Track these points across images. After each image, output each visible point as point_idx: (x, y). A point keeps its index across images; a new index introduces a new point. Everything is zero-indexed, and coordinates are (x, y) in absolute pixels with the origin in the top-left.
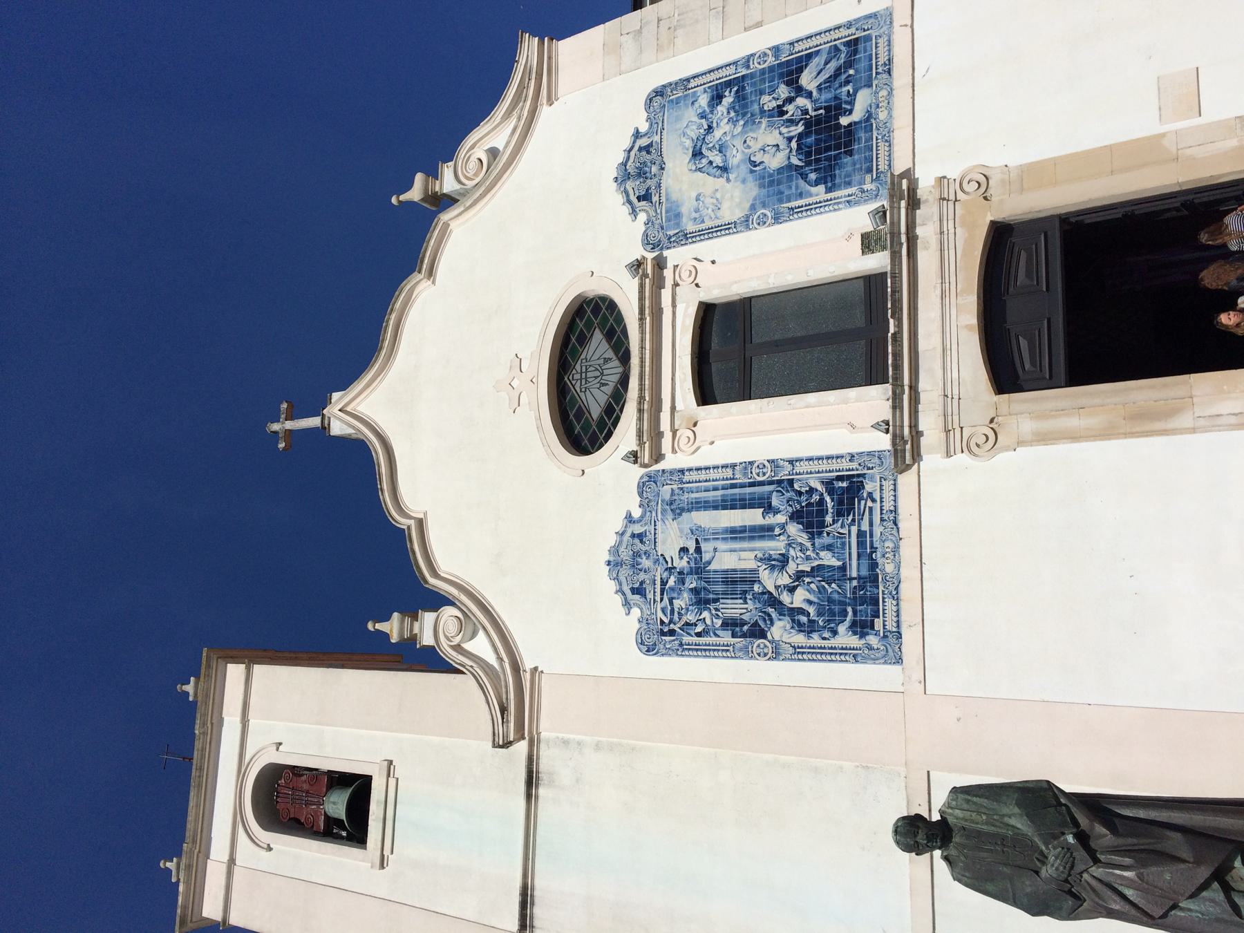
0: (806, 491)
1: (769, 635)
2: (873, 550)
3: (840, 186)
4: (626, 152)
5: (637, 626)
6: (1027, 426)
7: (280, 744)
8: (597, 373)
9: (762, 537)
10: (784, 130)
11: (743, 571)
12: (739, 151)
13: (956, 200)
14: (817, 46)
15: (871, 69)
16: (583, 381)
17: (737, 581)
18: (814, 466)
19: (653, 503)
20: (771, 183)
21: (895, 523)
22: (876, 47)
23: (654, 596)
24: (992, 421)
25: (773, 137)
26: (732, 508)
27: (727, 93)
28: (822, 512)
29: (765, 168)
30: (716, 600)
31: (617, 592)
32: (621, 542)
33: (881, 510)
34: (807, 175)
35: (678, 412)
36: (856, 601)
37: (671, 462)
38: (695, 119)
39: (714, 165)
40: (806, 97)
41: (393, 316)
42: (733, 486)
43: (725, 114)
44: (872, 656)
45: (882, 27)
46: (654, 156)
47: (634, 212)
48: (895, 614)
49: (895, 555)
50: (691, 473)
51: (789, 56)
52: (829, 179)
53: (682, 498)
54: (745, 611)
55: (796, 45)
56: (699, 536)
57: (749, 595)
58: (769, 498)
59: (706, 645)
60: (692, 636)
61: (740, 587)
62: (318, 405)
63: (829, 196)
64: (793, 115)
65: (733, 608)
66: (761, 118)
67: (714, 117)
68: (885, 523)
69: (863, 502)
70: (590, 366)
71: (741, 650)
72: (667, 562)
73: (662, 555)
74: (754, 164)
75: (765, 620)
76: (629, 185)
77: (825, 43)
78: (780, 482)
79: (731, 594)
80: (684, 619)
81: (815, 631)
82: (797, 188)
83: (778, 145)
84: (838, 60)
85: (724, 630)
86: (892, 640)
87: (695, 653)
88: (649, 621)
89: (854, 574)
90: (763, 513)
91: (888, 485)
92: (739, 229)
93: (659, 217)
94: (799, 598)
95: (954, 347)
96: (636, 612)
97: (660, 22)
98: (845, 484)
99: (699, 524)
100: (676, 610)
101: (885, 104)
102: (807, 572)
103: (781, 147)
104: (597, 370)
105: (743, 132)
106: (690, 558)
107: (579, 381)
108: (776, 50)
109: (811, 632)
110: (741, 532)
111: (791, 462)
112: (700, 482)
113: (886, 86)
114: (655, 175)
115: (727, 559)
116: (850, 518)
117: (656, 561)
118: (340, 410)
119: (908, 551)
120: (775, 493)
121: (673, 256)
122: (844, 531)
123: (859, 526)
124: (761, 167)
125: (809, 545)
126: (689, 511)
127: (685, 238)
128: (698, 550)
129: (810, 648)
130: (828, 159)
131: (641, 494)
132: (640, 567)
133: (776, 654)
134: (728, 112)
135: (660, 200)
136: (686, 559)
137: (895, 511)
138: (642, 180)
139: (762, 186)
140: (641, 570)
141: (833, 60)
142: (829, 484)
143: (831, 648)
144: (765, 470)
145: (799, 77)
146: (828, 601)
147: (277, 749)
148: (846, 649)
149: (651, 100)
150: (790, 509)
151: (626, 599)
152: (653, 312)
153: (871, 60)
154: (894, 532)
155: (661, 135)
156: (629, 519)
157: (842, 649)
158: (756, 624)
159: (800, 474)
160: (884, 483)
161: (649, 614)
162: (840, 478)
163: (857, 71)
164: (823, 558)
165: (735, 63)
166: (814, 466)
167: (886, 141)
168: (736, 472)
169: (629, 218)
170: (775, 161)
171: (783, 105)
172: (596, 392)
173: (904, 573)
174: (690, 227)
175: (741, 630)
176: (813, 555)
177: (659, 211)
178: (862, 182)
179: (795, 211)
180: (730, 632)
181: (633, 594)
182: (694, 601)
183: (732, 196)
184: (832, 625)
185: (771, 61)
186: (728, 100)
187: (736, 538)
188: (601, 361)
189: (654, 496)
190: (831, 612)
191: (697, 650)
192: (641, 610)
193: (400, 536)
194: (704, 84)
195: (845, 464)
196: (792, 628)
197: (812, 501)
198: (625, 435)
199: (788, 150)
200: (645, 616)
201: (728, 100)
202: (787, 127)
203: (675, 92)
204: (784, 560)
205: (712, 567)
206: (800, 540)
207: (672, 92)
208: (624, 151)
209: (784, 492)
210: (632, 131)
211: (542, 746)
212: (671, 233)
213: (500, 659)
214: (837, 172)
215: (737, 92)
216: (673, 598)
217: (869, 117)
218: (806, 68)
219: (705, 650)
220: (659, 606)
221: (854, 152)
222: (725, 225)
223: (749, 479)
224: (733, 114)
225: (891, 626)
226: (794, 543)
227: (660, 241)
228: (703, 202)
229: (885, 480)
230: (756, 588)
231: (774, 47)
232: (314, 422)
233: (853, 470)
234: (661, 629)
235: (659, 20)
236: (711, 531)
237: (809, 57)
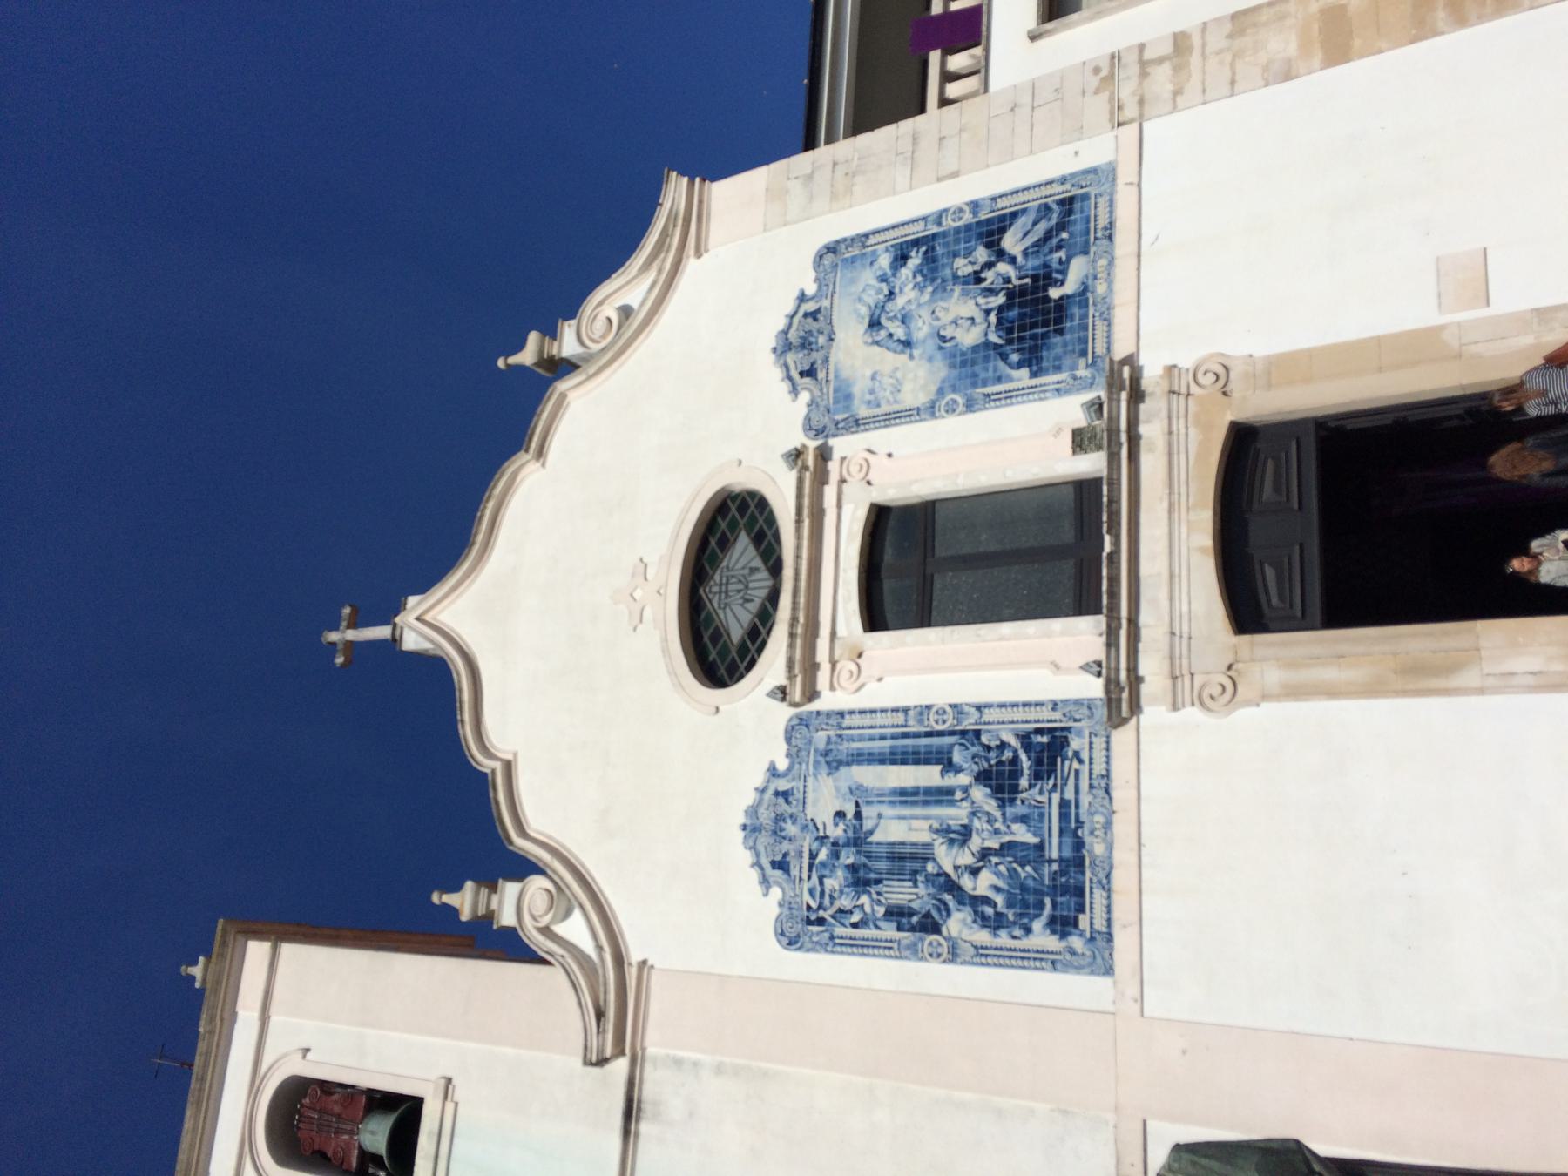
0: (997, 746)
1: (944, 930)
2: (1079, 825)
4: (788, 319)
5: (776, 910)
6: (1273, 676)
7: (307, 1050)
8: (740, 586)
9: (939, 803)
10: (981, 300)
11: (914, 844)
12: (927, 323)
13: (1188, 395)
14: (1024, 203)
15: (1087, 232)
16: (723, 596)
17: (906, 858)
18: (1007, 715)
19: (804, 753)
20: (964, 364)
21: (1107, 791)
22: (1096, 208)
23: (800, 872)
24: (1230, 667)
25: (968, 308)
27: (913, 254)
28: (1016, 774)
29: (956, 345)
30: (878, 882)
31: (753, 866)
33: (1091, 774)
34: (1007, 355)
35: (840, 638)
36: (1055, 890)
37: (828, 701)
38: (874, 282)
39: (895, 338)
40: (1009, 263)
41: (491, 505)
42: (905, 735)
44: (1075, 964)
45: (1103, 184)
46: (821, 323)
47: (795, 390)
48: (1105, 909)
49: (1106, 833)
50: (853, 716)
51: (991, 212)
52: (1034, 361)
53: (840, 748)
54: (914, 897)
55: (998, 200)
56: (860, 796)
57: (921, 876)
58: (950, 752)
59: (863, 939)
60: (845, 926)
61: (909, 866)
62: (389, 611)
63: (1035, 381)
64: (992, 283)
65: (900, 893)
66: (954, 285)
67: (896, 281)
68: (1094, 791)
69: (1067, 763)
70: (733, 576)
71: (908, 947)
72: (817, 829)
73: (812, 820)
74: (944, 339)
75: (939, 910)
77: (1034, 200)
78: (963, 733)
79: (898, 874)
80: (838, 904)
81: (1003, 927)
82: (995, 370)
83: (972, 319)
84: (1049, 219)
85: (887, 920)
86: (1100, 942)
88: (793, 905)
89: (1055, 855)
90: (942, 771)
91: (1099, 743)
92: (923, 416)
93: (825, 397)
94: (983, 884)
95: (1184, 573)
96: (776, 893)
97: (837, 167)
98: (1045, 739)
100: (827, 892)
102: (996, 850)
103: (978, 320)
104: (740, 581)
105: (931, 301)
106: (847, 826)
107: (717, 596)
108: (975, 206)
111: (979, 708)
112: (863, 728)
113: (1105, 255)
114: (822, 347)
116: (1051, 782)
117: (804, 828)
118: (418, 619)
119: (1123, 827)
120: (957, 748)
121: (841, 445)
122: (1044, 798)
123: (1062, 792)
125: (998, 814)
126: (848, 764)
127: (856, 424)
128: (858, 815)
129: (996, 949)
130: (1034, 337)
131: (788, 740)
133: (954, 955)
134: (914, 277)
135: (827, 377)
136: (842, 826)
137: (1107, 776)
138: (806, 352)
139: (952, 366)
140: (784, 838)
141: (1043, 221)
142: (1025, 738)
143: (1024, 951)
144: (945, 717)
145: (1000, 240)
146: (1021, 890)
147: (304, 1057)
148: (1043, 952)
149: (821, 257)
150: (976, 768)
151: (764, 876)
152: (813, 513)
154: (1106, 802)
155: (832, 299)
156: (773, 772)
157: (1038, 952)
158: (928, 915)
159: (989, 723)
160: (1094, 739)
161: (792, 894)
162: (1039, 731)
163: (1071, 235)
164: (1016, 832)
165: (924, 219)
166: (1007, 715)
167: (1105, 320)
168: (909, 718)
169: (789, 397)
170: (969, 337)
172: (738, 609)
173: (1118, 856)
174: (863, 412)
175: (909, 922)
176: (1003, 828)
177: (825, 390)
178: (1074, 367)
179: (993, 397)
180: (894, 925)
181: (774, 868)
182: (850, 880)
183: (916, 376)
184: (1025, 920)
185: (968, 218)
186: (915, 260)
188: (746, 571)
189: (805, 744)
190: (1025, 903)
191: (852, 946)
192: (783, 889)
193: (482, 782)
194: (886, 241)
196: (975, 921)
197: (1004, 758)
198: (772, 665)
199: (986, 324)
200: (787, 898)
201: (915, 260)
202: (985, 297)
203: (850, 249)
204: (966, 833)
205: (874, 838)
206: (987, 808)
207: (846, 249)
209: (969, 746)
210: (796, 294)
211: (648, 1068)
212: (839, 417)
213: (599, 948)
214: (1045, 354)
215: (926, 252)
217: (1085, 290)
219: (862, 946)
220: (806, 886)
221: (1066, 330)
222: (906, 411)
223: (925, 727)
224: (919, 279)
225: (1100, 925)
226: (979, 812)
227: (825, 427)
228: (880, 382)
229: (1096, 735)
230: (930, 867)
231: (972, 202)
232: (383, 632)
233: (1055, 721)
234: (807, 917)
235: (835, 164)
236: (875, 792)
237: (1014, 215)
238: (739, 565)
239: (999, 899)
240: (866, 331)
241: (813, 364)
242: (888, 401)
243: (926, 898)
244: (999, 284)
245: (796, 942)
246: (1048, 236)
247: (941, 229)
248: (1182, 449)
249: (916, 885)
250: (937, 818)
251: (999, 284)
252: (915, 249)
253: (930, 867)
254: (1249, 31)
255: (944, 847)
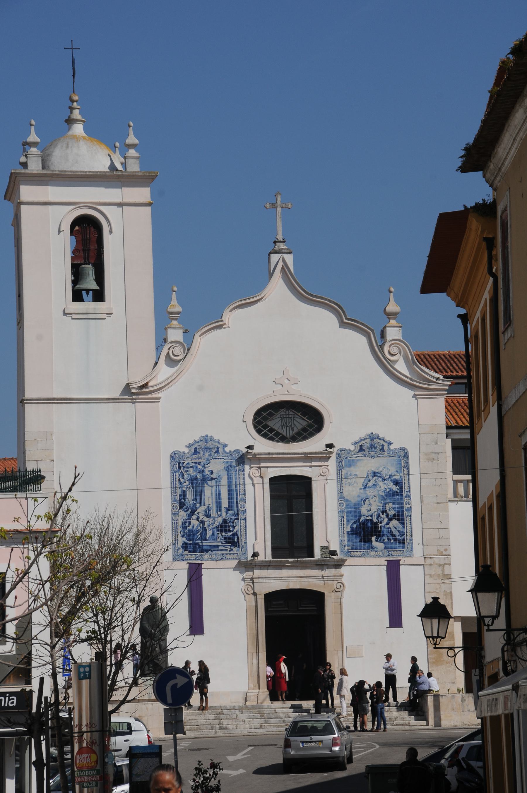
1: (181, 510)
3: (349, 537)
5: (181, 451)
9: (217, 507)
10: (376, 513)
15: (391, 549)
16: (285, 416)
18: (243, 528)
26: (228, 494)
27: (397, 487)
30: (193, 488)
32: (215, 442)
36: (194, 544)
39: (368, 482)
43: (389, 487)
46: (379, 453)
47: (356, 443)
53: (233, 471)
58: (232, 510)
61: (198, 497)
63: (346, 533)
65: (190, 495)
69: (229, 547)
70: (291, 420)
72: (207, 464)
74: (365, 501)
75: (186, 508)
76: (368, 441)
78: (238, 514)
80: (185, 473)
82: (352, 519)
83: (370, 511)
86: (181, 558)
87: (172, 478)
89: (204, 544)
91: (235, 556)
94: (195, 522)
96: (186, 450)
98: (236, 540)
99: (223, 479)
101: (376, 554)
103: (369, 512)
105: (379, 495)
107: (285, 414)
108: (410, 509)
109: (183, 527)
110: (219, 498)
111: (245, 519)
115: (209, 492)
116: (224, 542)
117: (208, 460)
122: (219, 540)
123: (221, 546)
124: (363, 504)
125: (214, 526)
126: (228, 474)
127: (340, 469)
128: (212, 479)
129: (177, 527)
130: (360, 532)
131: (235, 451)
132: (205, 451)
133: (174, 514)
134: (389, 488)
139: (355, 504)
140: (204, 452)
142: (236, 534)
149: (404, 450)
151: (192, 445)
153: (395, 549)
154: (219, 559)
156: (225, 446)
158: (185, 505)
160: (236, 555)
162: (238, 538)
163: (392, 543)
166: (243, 528)
169: (353, 441)
170: (364, 510)
171: (386, 513)
174: (344, 472)
176: (210, 528)
177: (354, 456)
178: (348, 546)
181: (194, 449)
182: (193, 478)
185: (406, 507)
186: (395, 488)
187: (217, 496)
190: (190, 535)
191: (174, 479)
192: (188, 453)
195: (243, 540)
196: (184, 520)
201: (395, 488)
204: (208, 516)
205: (205, 485)
208: (384, 437)
215: (397, 492)
216: (193, 467)
218: (399, 522)
220: (190, 461)
221: (361, 543)
224: (388, 490)
227: (341, 457)
230: (198, 505)
231: (411, 508)
237: (403, 524)
238: (295, 423)
239: (190, 527)
240: (373, 471)
241: (364, 450)
242: (346, 481)
243: (189, 504)
244: (381, 519)
245: (173, 459)
246: (393, 535)
247: (404, 497)
248: (318, 580)
249: (192, 500)
250: (212, 506)
251: (381, 519)
252: (399, 488)
253: (198, 505)
254: (445, 597)
255: (204, 509)
